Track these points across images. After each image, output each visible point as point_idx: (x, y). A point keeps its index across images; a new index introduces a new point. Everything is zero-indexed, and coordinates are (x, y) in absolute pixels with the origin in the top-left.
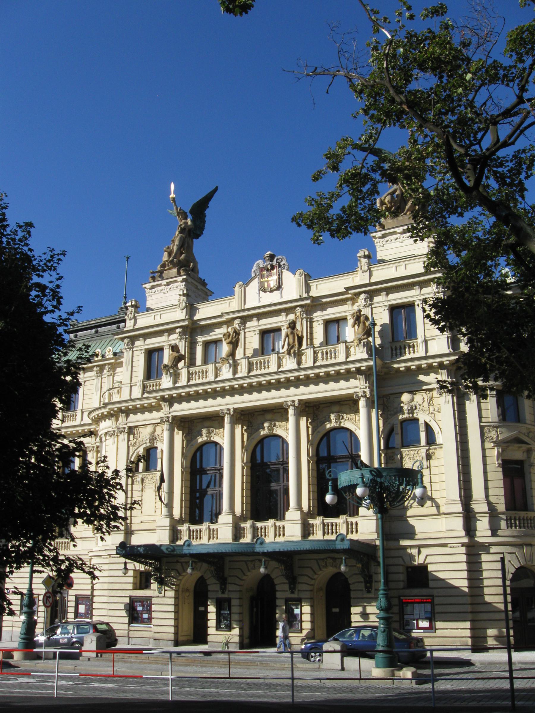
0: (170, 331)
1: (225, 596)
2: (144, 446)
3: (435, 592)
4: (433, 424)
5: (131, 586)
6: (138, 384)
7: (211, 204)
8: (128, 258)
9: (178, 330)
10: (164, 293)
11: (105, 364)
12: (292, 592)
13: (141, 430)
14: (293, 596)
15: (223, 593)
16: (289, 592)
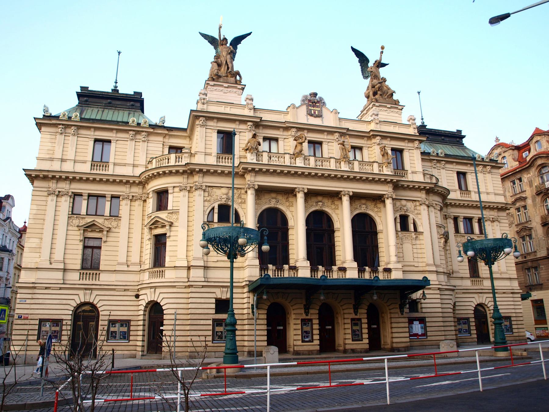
0: (244, 122)
1: (308, 317)
2: (219, 203)
3: (426, 315)
4: (416, 220)
5: (213, 311)
6: (213, 155)
7: (243, 42)
8: (119, 53)
9: (249, 123)
10: (224, 93)
11: (143, 131)
12: (356, 315)
13: (215, 190)
14: (356, 317)
15: (307, 315)
16: (354, 315)
